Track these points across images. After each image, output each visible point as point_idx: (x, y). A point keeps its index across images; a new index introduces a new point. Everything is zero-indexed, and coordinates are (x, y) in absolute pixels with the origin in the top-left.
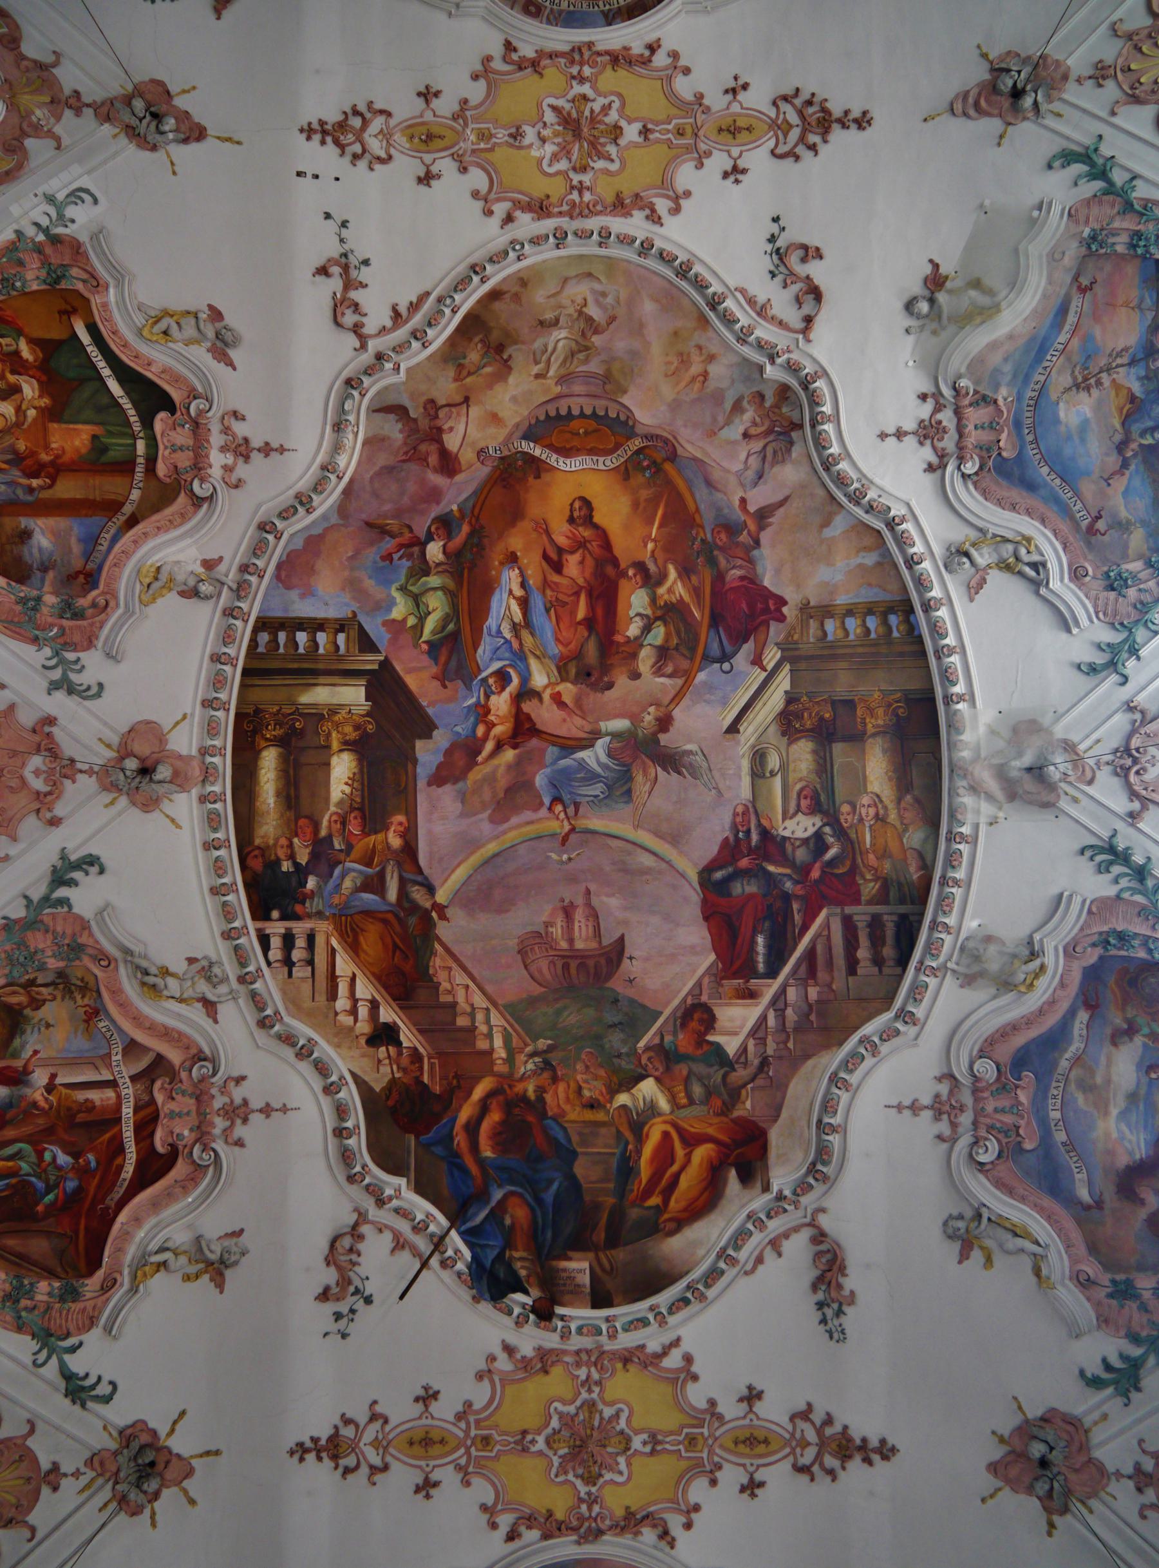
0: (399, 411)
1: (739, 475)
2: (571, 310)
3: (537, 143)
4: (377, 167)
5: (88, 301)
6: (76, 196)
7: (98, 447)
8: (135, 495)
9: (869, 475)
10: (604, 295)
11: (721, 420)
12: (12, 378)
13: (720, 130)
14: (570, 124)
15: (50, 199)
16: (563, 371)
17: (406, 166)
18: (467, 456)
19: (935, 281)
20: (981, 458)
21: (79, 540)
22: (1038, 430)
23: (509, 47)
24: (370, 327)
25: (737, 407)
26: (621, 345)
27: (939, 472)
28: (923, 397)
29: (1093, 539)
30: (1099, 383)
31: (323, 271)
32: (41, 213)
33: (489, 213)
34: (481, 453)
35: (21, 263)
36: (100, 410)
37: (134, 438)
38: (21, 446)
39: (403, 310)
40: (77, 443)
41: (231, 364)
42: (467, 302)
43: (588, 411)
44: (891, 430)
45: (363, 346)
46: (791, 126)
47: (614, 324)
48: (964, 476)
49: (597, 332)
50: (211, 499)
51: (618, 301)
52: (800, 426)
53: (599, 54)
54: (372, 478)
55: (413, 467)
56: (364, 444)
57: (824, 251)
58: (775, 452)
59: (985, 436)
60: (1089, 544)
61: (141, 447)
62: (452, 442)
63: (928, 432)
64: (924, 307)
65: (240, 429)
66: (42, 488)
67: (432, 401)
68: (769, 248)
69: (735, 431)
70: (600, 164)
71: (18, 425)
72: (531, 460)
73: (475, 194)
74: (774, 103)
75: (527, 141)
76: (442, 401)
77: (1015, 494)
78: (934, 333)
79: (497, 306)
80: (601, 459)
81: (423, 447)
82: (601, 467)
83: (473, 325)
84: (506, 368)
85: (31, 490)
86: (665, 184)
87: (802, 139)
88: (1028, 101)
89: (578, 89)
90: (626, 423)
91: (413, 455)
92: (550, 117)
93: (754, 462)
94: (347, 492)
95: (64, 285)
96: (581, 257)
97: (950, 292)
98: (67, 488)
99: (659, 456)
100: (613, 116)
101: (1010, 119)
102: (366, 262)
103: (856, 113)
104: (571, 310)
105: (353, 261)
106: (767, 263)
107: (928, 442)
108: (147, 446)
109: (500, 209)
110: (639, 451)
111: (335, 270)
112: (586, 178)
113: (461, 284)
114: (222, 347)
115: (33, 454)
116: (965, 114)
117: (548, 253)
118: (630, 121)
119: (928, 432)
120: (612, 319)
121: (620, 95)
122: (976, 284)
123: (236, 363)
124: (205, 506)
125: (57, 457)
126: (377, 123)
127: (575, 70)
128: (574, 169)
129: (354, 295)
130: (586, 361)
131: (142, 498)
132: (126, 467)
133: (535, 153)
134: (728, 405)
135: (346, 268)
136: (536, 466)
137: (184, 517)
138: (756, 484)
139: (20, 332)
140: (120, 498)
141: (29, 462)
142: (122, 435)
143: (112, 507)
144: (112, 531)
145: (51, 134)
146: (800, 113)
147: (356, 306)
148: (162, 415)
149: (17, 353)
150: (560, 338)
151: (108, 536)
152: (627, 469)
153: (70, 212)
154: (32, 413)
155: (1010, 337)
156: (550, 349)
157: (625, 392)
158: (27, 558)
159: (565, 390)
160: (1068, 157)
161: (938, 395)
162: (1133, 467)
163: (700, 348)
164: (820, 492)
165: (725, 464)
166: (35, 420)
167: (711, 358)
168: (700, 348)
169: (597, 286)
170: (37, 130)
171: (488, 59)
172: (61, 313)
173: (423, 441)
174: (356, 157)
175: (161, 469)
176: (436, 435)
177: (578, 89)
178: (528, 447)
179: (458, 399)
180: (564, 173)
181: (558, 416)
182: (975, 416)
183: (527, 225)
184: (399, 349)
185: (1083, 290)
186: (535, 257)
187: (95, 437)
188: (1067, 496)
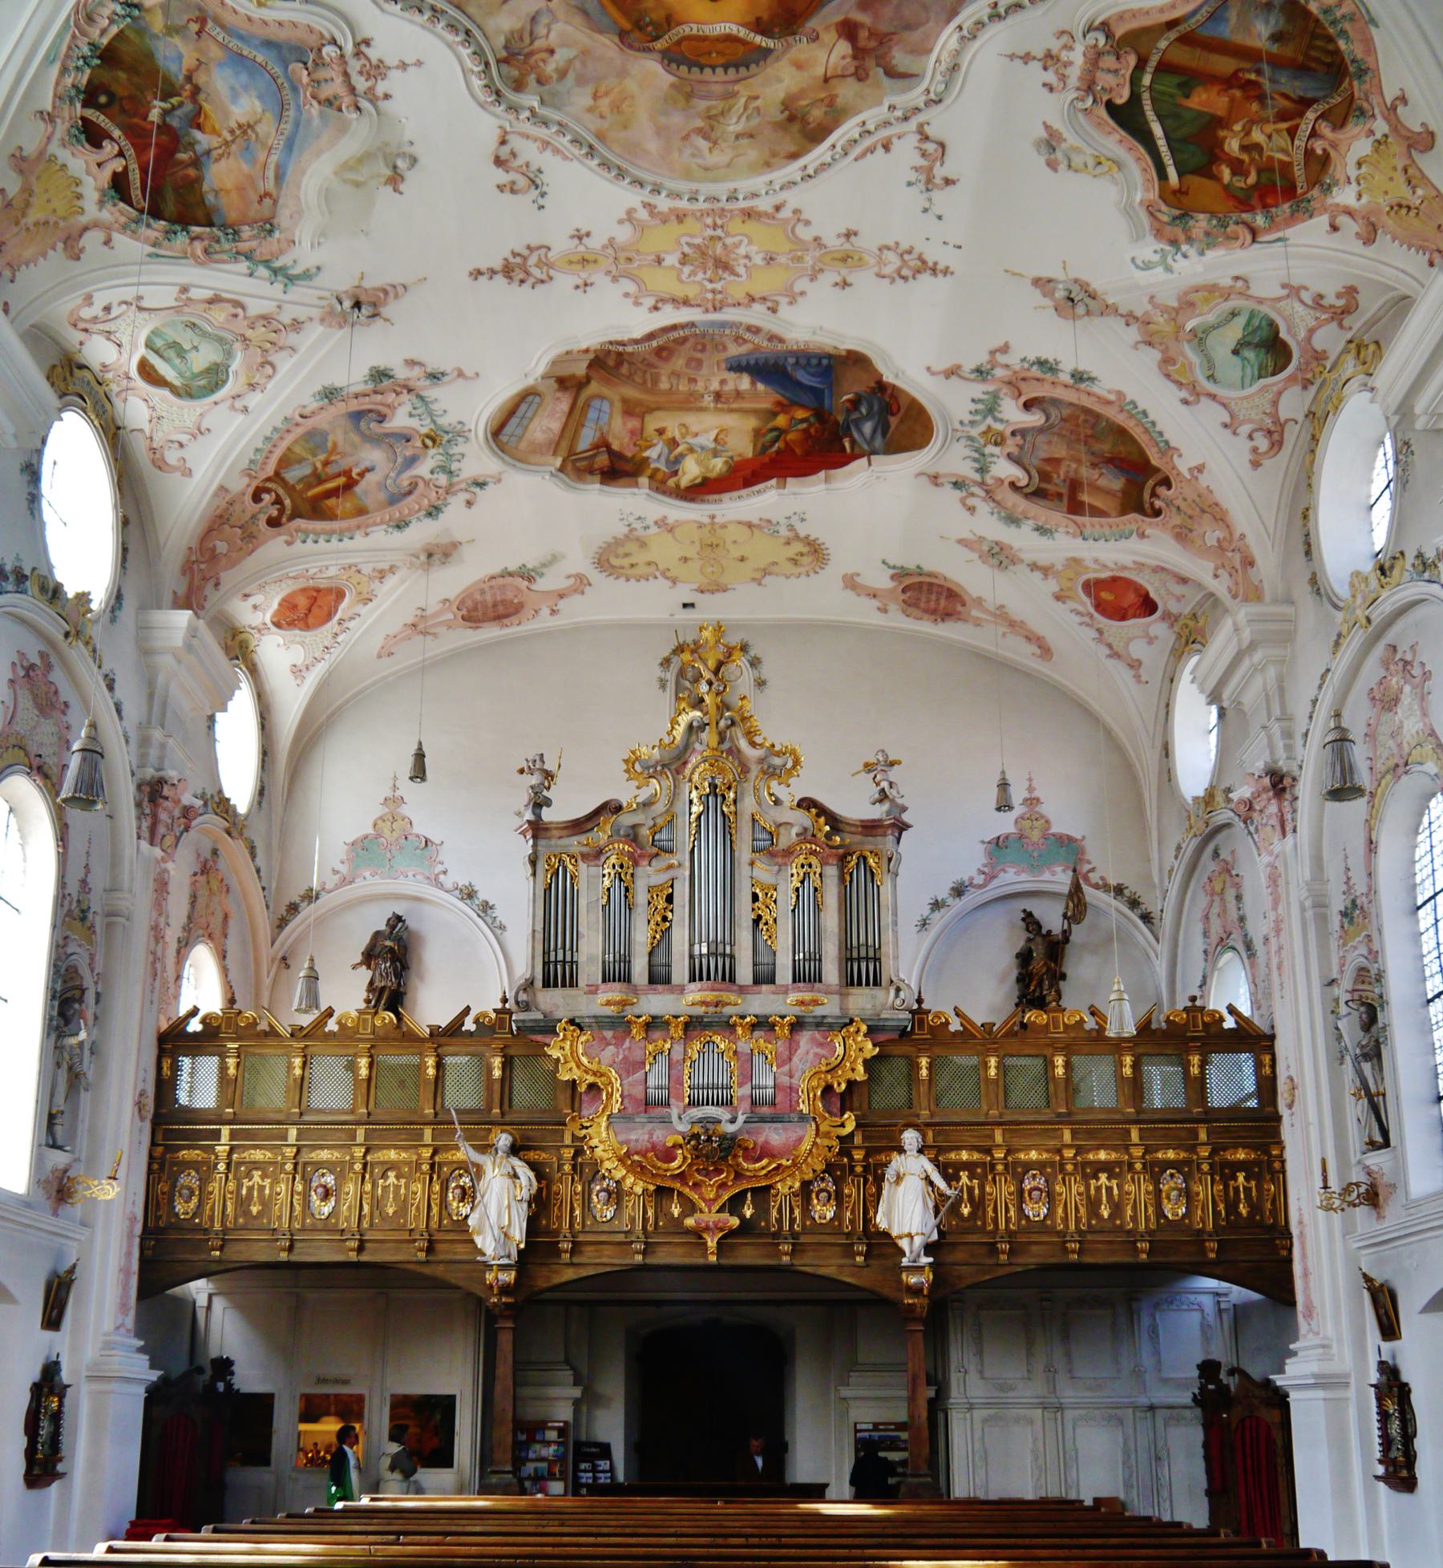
0: (892, 73)
1: (555, 19)
2: (724, 145)
3: (752, 255)
4: (891, 244)
5: (1161, 197)
6: (1147, 266)
7: (1186, 89)
8: (1163, 44)
9: (426, 33)
10: (693, 156)
11: (577, 64)
12: (1245, 157)
13: (595, 261)
14: (723, 265)
15: (1169, 269)
16: (731, 101)
17: (868, 242)
18: (829, 37)
19: (395, 180)
20: (321, 58)
21: (1227, 20)
22: (274, 87)
23: (774, 311)
24: (913, 140)
25: (563, 74)
26: (677, 119)
27: (359, 39)
28: (387, 97)
29: (197, 13)
30: (232, 132)
31: (948, 182)
32: (1181, 264)
33: (796, 211)
34: (815, 38)
35: (1207, 234)
36: (1176, 116)
37: (1150, 88)
38: (1255, 106)
39: (880, 150)
40: (1204, 96)
41: (1047, 127)
42: (820, 153)
43: (708, 71)
44: (411, 70)
45: (921, 126)
46: (537, 266)
47: (684, 133)
48: (334, 42)
49: (699, 131)
50: (1090, 28)
51: (680, 151)
52: (498, 61)
53: (699, 306)
54: (927, 21)
55: (883, 27)
56: (930, 51)
57: (497, 191)
58: (521, 39)
59: (322, 74)
60: (200, 9)
61: (1147, 80)
62: (844, 48)
63: (377, 70)
64: (400, 163)
65: (1050, 77)
66: (1249, 71)
67: (860, 80)
68: (545, 189)
69: (562, 56)
70: (698, 241)
71: (1252, 122)
72: (764, 32)
73: (807, 223)
74: (551, 278)
75: (761, 256)
76: (851, 80)
77: (281, 35)
78: (387, 144)
79: (793, 148)
80: (695, 31)
81: (872, 44)
82: (695, 27)
83: (816, 135)
84: (786, 105)
85: (1259, 72)
86: (640, 228)
87: (525, 259)
88: (347, 304)
89: (718, 286)
90: (670, 61)
91: (883, 39)
92: (741, 270)
93: (541, 30)
94: (953, 13)
95: (1177, 212)
96: (715, 181)
97: (379, 176)
98: (1225, 65)
99: (636, 35)
100: (687, 270)
101: (358, 291)
102: (909, 184)
103: (483, 279)
104: (724, 145)
105: (922, 186)
106: (545, 178)
107: (374, 62)
108: (1140, 80)
109: (785, 213)
110: (657, 38)
111: (938, 181)
112: (709, 232)
113: (823, 167)
114: (1051, 142)
115: (1248, 98)
116: (394, 287)
117: (745, 185)
118: (673, 267)
119: (377, 70)
120: (686, 138)
121: (681, 282)
122: (357, 185)
123: (1042, 127)
124: (1097, 23)
125: (1226, 90)
126: (888, 270)
127: (719, 297)
128: (720, 238)
129: (923, 162)
130: (709, 109)
131: (1157, 40)
132: (1165, 68)
133: (754, 248)
134: (571, 76)
135: (929, 181)
136: (760, 26)
137: (1121, 17)
138: (537, 12)
139: (1226, 188)
140: (1177, 44)
141: (1253, 93)
142: (1163, 93)
143: (1187, 40)
144: (1193, 20)
145: (1155, 306)
146: (528, 273)
147: (924, 155)
148: (1120, 101)
149: (1234, 173)
150: (734, 125)
151: (1198, 17)
152: (669, 24)
153: (1156, 258)
154: (1237, 127)
155: (318, 154)
156: (744, 118)
157: (673, 86)
158: (1282, 21)
159: (730, 88)
160: (306, 276)
161: (373, 100)
162: (181, 78)
163: (602, 117)
164: (471, 10)
165: (570, 29)
166: (1237, 122)
167: (590, 110)
168: (602, 117)
169: (700, 161)
170: (1165, 310)
171: (791, 303)
172: (1186, 193)
173: (873, 49)
174: (910, 252)
175: (1132, 60)
176: (859, 53)
177: (718, 286)
178: (770, 43)
179: (833, 82)
180: (728, 234)
181: (737, 66)
182: (336, 87)
183: (764, 204)
184: (887, 124)
185: (267, 194)
186: (758, 182)
187: (1187, 96)
188: (234, 43)
